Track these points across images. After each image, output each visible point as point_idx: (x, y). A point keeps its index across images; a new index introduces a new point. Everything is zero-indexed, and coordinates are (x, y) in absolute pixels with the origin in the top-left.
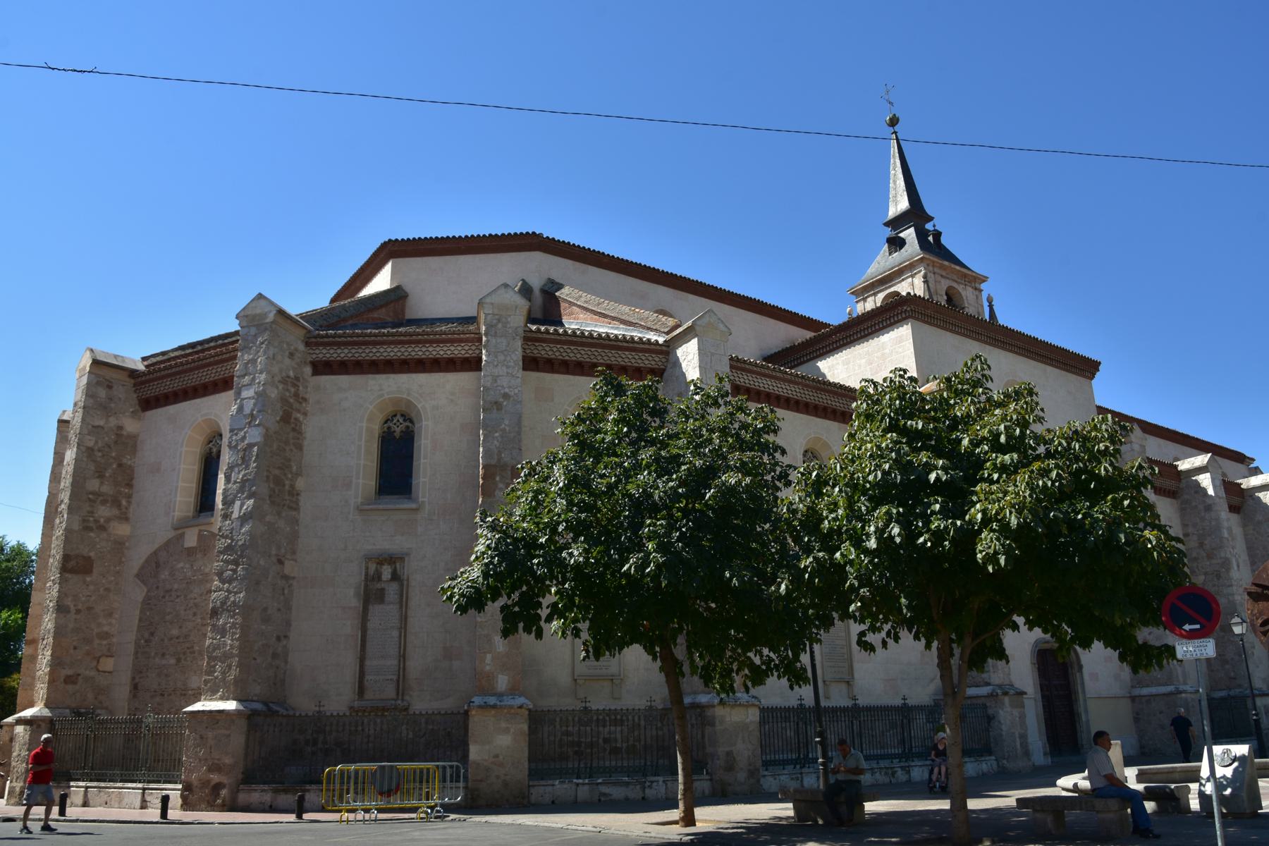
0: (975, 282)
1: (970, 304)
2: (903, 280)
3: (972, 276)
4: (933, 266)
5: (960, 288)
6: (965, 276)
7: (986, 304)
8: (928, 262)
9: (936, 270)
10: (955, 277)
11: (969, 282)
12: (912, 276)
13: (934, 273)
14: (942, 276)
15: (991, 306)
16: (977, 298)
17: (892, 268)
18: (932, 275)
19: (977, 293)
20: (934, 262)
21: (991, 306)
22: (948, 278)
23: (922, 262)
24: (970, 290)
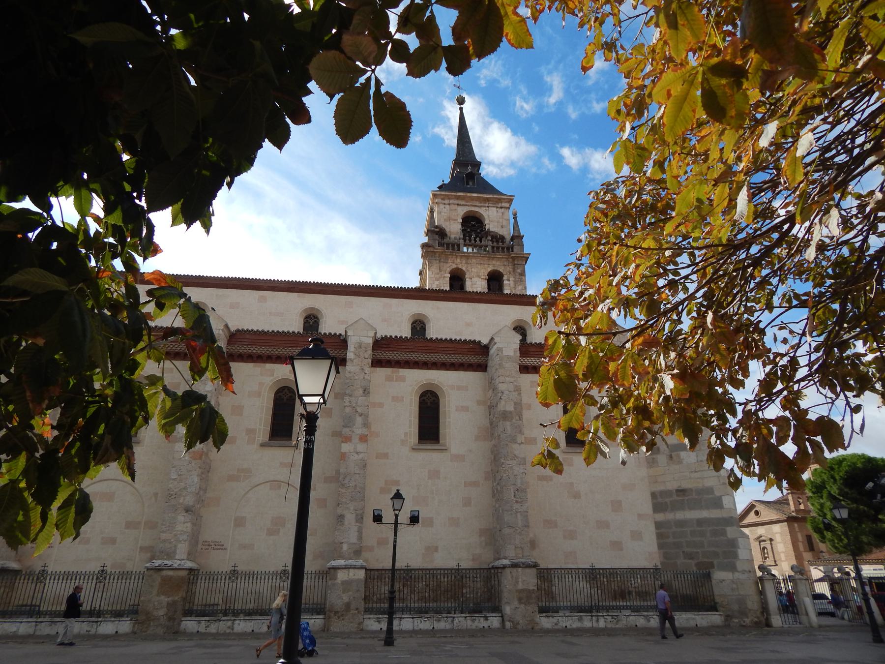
5: (482, 211)
8: (442, 197)
9: (452, 201)
10: (477, 204)
14: (458, 205)
15: (515, 218)
16: (503, 213)
18: (447, 206)
20: (446, 195)
21: (515, 218)
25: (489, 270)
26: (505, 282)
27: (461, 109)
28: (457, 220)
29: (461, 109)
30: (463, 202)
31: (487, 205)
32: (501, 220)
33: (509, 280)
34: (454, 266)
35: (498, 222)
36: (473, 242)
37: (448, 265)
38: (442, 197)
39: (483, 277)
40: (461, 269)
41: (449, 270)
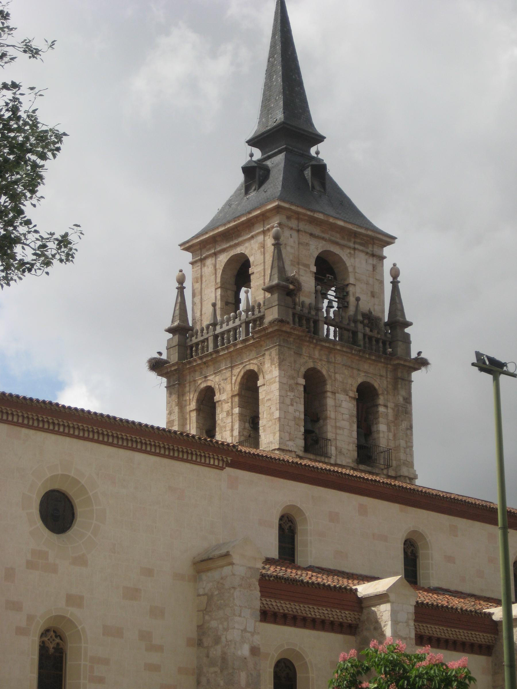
0: (373, 244)
2: (252, 237)
3: (367, 236)
4: (298, 219)
5: (344, 254)
6: (355, 235)
7: (388, 279)
9: (302, 226)
10: (337, 237)
11: (361, 244)
12: (264, 232)
13: (298, 231)
14: (311, 235)
15: (395, 284)
16: (374, 267)
17: (239, 217)
18: (295, 234)
19: (375, 261)
20: (298, 213)
21: (395, 284)
22: (323, 239)
23: (278, 212)
24: (362, 257)
25: (360, 380)
26: (381, 409)
30: (317, 231)
32: (371, 281)
33: (386, 406)
34: (311, 365)
35: (367, 284)
37: (302, 361)
39: (351, 394)
40: (319, 372)
41: (303, 370)
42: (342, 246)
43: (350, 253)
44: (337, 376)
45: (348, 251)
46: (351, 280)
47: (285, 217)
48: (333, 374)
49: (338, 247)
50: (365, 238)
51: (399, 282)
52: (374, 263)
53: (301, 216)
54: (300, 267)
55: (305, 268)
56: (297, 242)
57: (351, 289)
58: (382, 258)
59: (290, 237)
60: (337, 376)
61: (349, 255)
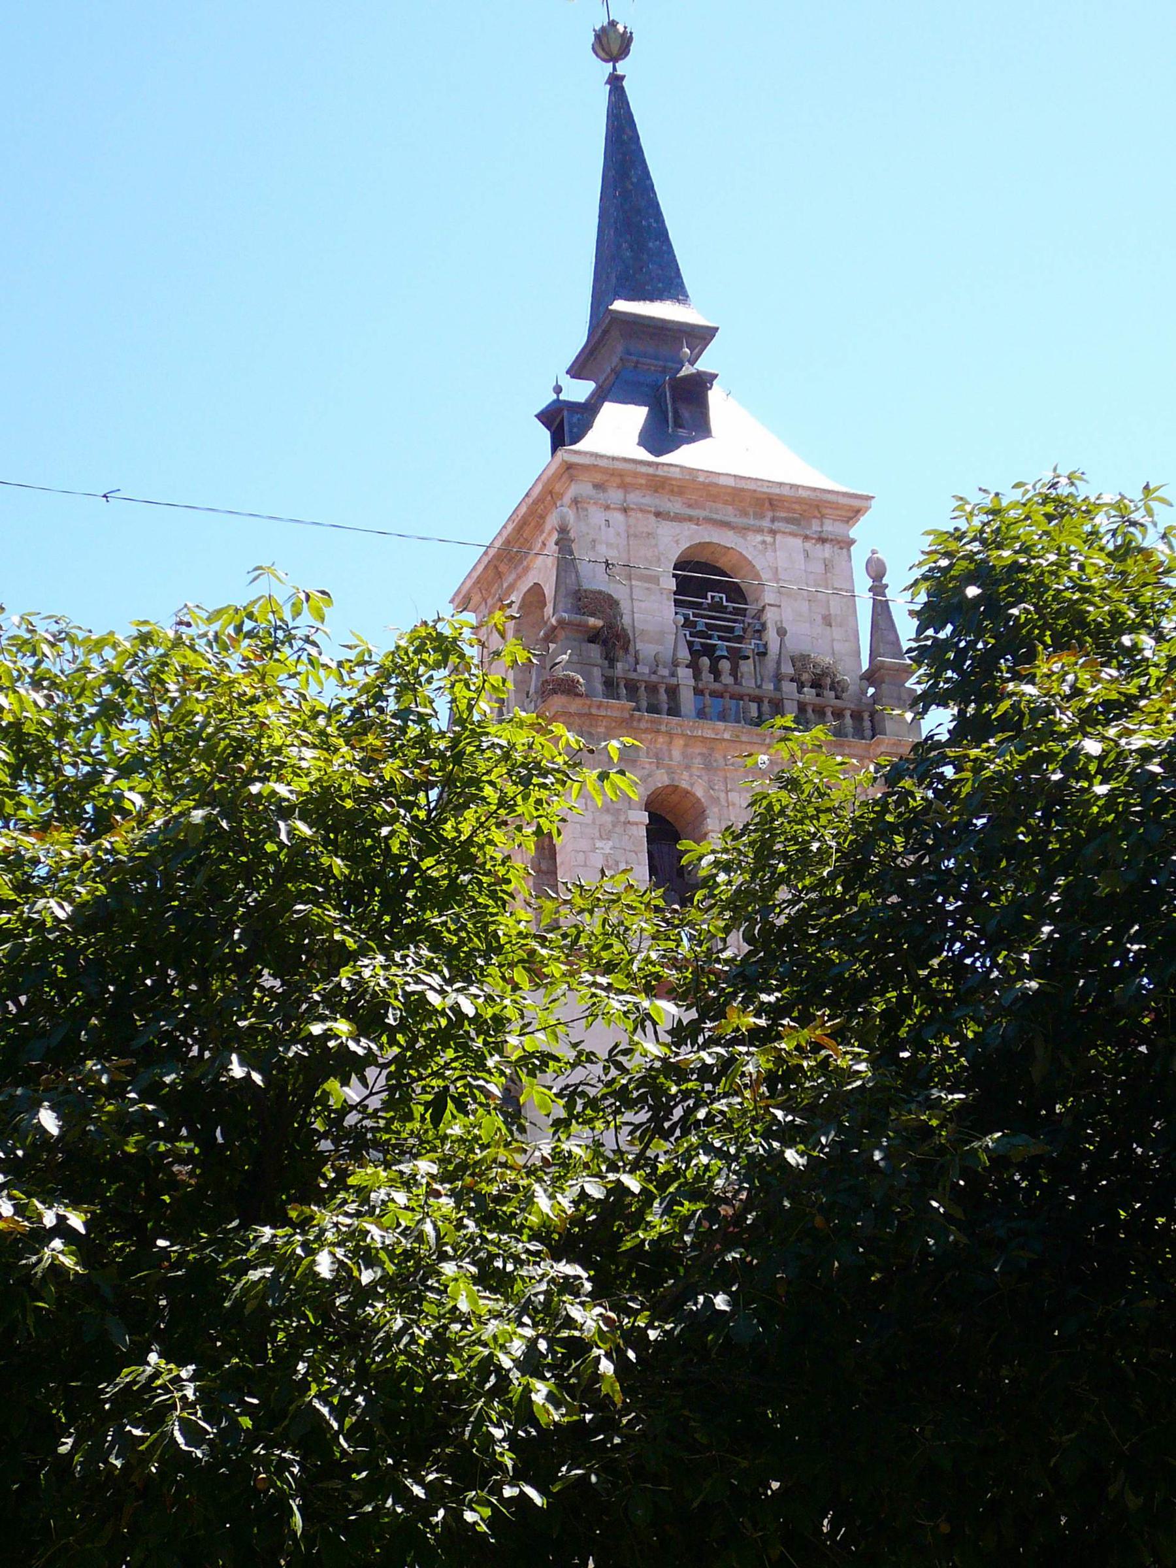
0: (823, 516)
1: (790, 594)
4: (624, 487)
7: (862, 583)
9: (634, 498)
10: (728, 513)
11: (788, 521)
13: (625, 510)
16: (828, 566)
18: (618, 517)
19: (827, 551)
22: (690, 519)
23: (572, 479)
27: (616, 82)
28: (655, 580)
29: (616, 82)
30: (675, 506)
31: (766, 523)
36: (727, 679)
38: (598, 478)
42: (743, 530)
43: (764, 542)
44: (733, 796)
45: (759, 538)
46: (769, 597)
47: (590, 486)
48: (722, 795)
49: (730, 533)
50: (797, 507)
51: (886, 586)
52: (827, 555)
53: (628, 480)
54: (634, 583)
55: (646, 585)
56: (624, 535)
57: (770, 616)
58: (847, 544)
59: (603, 527)
60: (733, 796)
61: (760, 547)
